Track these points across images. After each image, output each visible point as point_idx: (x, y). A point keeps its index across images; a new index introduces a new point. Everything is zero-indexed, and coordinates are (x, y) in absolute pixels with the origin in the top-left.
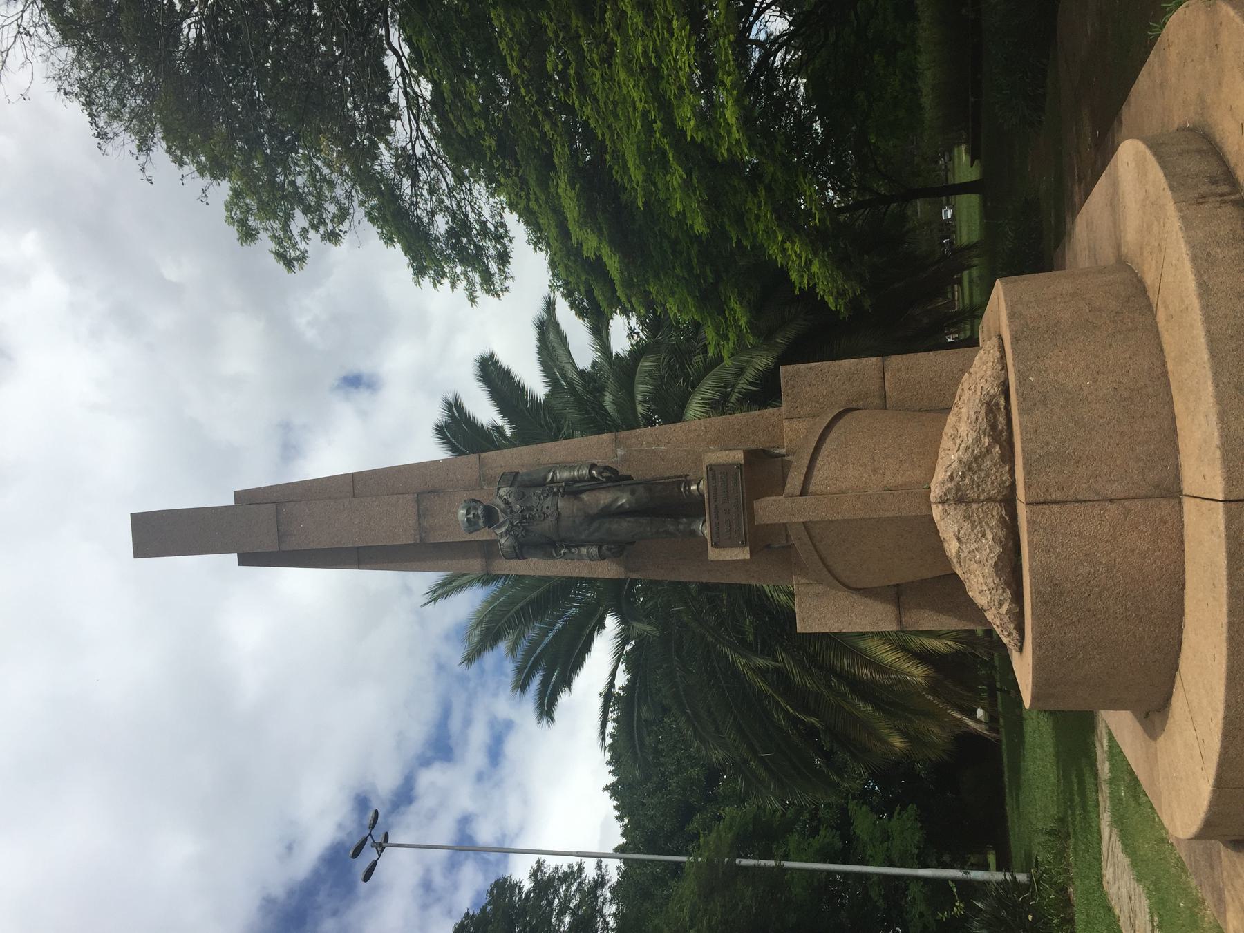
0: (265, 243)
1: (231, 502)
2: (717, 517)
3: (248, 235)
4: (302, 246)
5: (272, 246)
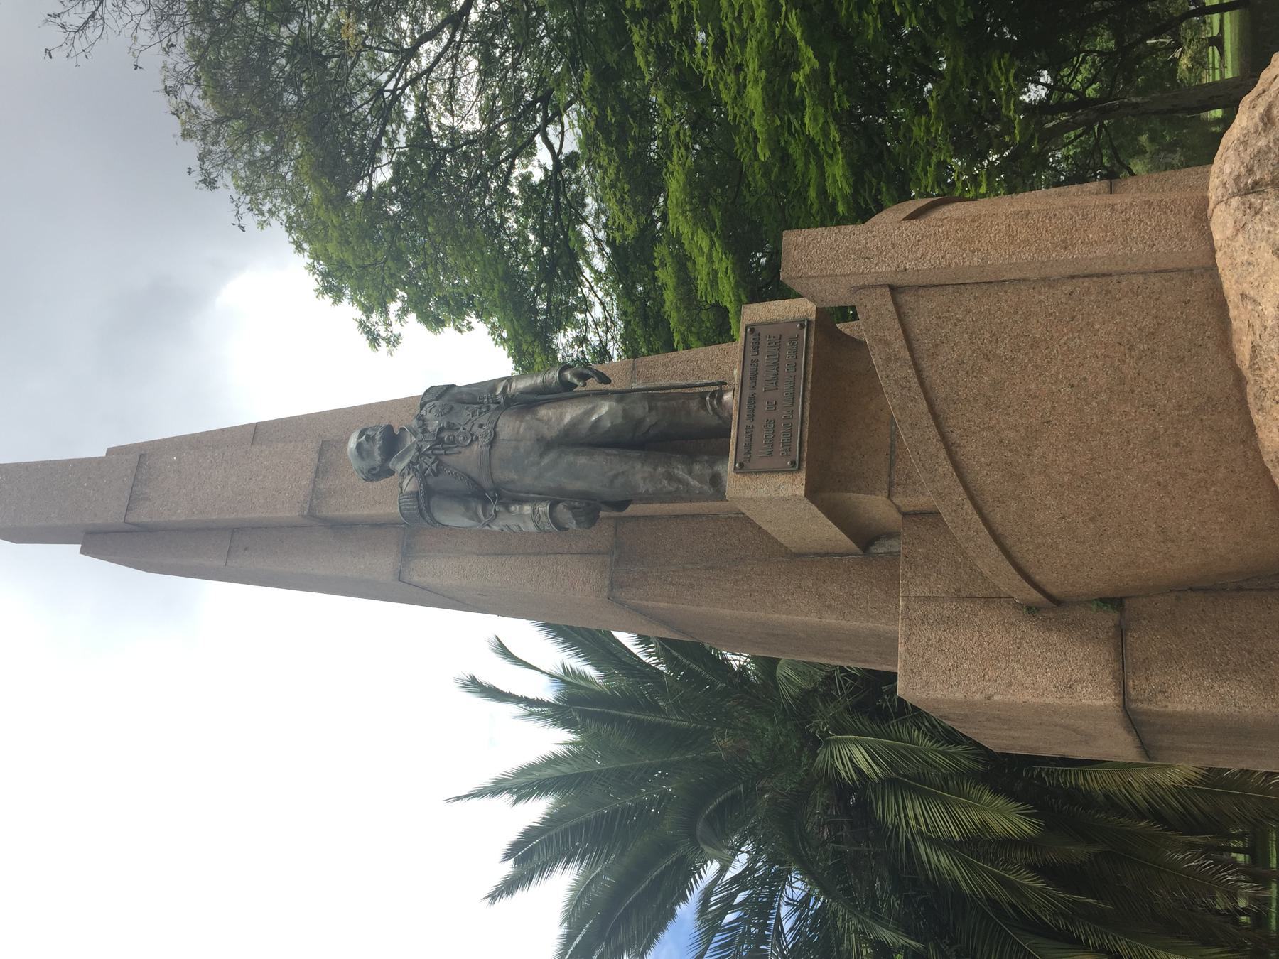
2: (752, 417)
4: (396, 328)
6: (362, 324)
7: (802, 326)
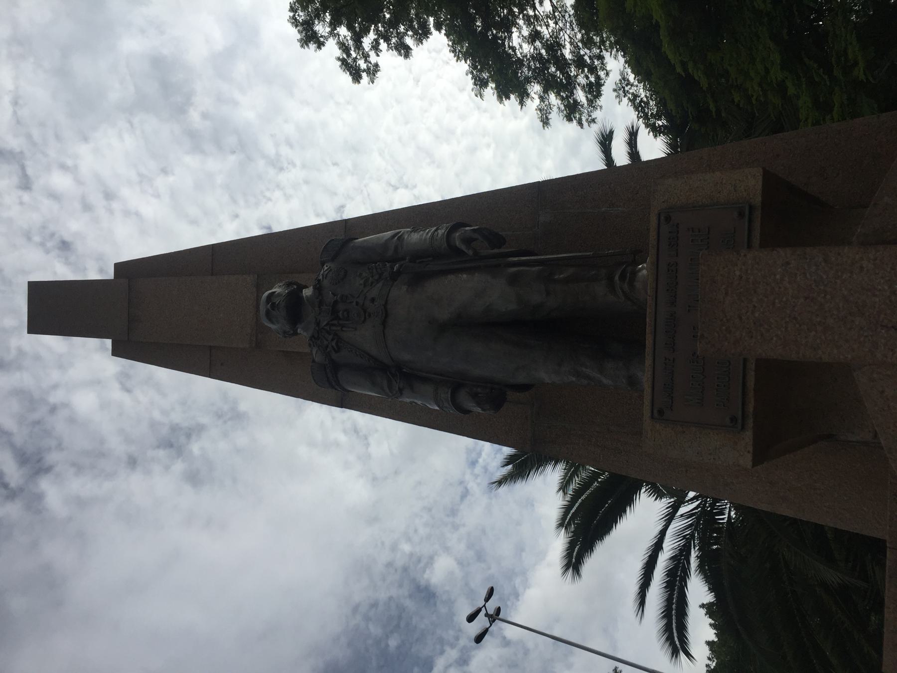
0: (332, 48)
1: (110, 275)
3: (310, 37)
4: (373, 58)
5: (338, 53)
6: (344, 62)
7: (741, 215)
